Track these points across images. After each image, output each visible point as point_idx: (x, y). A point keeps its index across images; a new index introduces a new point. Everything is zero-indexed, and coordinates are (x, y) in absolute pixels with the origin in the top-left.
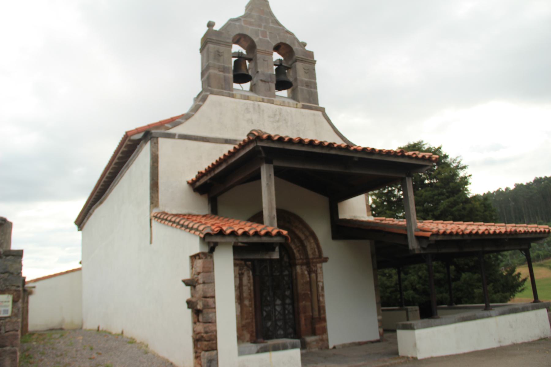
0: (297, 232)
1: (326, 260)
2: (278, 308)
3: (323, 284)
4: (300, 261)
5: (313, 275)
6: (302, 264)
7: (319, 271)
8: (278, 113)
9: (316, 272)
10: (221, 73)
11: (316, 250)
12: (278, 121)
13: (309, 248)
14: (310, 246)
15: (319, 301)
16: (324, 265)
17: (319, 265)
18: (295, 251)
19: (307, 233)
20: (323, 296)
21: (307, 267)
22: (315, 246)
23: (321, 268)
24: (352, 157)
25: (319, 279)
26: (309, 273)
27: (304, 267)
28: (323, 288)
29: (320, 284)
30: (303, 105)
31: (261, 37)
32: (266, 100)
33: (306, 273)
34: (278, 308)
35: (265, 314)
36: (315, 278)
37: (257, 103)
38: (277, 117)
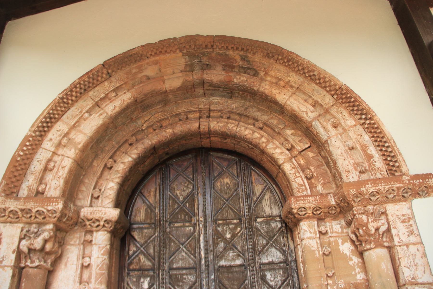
0: (282, 97)
4: (311, 203)
6: (320, 215)
7: (400, 233)
9: (385, 239)
11: (372, 150)
13: (337, 147)
14: (343, 140)
17: (391, 208)
18: (287, 168)
19: (328, 100)
21: (349, 224)
22: (367, 138)
23: (408, 220)
26: (359, 245)
33: (346, 248)
36: (386, 266)
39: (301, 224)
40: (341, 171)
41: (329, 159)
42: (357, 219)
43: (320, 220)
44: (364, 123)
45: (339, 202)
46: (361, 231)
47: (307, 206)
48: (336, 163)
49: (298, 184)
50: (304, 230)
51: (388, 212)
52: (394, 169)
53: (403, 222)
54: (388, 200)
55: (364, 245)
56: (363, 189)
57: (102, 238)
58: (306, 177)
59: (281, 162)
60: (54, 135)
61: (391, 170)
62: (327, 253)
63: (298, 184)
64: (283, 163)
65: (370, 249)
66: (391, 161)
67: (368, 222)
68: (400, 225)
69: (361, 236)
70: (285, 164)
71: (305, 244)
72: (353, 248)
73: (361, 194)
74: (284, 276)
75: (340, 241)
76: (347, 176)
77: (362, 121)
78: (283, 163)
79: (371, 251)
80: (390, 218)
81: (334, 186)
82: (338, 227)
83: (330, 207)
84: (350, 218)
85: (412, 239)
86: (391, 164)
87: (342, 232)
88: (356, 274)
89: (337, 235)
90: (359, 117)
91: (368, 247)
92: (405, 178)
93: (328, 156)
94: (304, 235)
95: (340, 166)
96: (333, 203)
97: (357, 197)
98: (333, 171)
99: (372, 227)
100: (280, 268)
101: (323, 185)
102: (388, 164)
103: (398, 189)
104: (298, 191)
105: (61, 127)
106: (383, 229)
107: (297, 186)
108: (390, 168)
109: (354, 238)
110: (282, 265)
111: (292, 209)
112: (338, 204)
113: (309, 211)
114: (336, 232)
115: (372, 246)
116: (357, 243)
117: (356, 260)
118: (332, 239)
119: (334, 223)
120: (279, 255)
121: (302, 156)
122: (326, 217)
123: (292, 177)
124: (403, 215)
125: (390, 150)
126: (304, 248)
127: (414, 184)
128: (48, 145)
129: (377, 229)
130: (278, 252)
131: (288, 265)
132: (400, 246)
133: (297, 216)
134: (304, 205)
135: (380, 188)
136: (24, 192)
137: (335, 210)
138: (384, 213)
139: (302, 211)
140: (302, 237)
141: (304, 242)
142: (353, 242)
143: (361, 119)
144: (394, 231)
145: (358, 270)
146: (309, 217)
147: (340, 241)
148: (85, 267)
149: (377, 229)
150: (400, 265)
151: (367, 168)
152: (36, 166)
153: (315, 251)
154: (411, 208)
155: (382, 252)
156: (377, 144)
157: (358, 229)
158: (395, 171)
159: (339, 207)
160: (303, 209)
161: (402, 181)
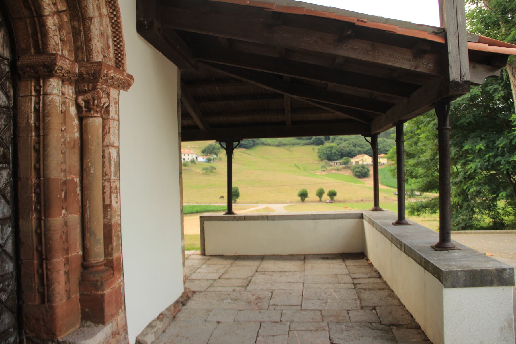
1: (126, 84)
5: (96, 122)
15: (107, 207)
20: (118, 190)
21: (78, 93)
23: (117, 103)
25: (112, 138)
27: (70, 91)
33: (73, 110)
39: (52, 80)
40: (93, 49)
41: (82, 33)
42: (98, 92)
43: (63, 81)
44: (112, 18)
45: (84, 73)
46: (96, 102)
47: (65, 66)
48: (91, 40)
49: (56, 43)
50: (54, 86)
51: (111, 94)
52: (120, 64)
53: (115, 103)
54: (112, 86)
55: (92, 112)
56: (110, 72)
58: (60, 38)
59: (47, 13)
61: (117, 64)
62: (63, 111)
63: (56, 43)
64: (49, 16)
65: (96, 117)
66: (120, 57)
67: (102, 97)
68: (113, 105)
69: (93, 104)
70: (50, 18)
71: (52, 99)
72: (76, 112)
73: (107, 75)
74: (7, 121)
75: (71, 104)
76: (97, 56)
77: (112, 16)
78: (49, 16)
79: (96, 119)
80: (111, 99)
81: (73, 55)
82: (71, 91)
83: (74, 73)
84: (87, 89)
85: (116, 117)
86: (120, 59)
87: (72, 97)
88: (75, 133)
89: (69, 98)
90: (111, 11)
91: (96, 115)
92: (125, 74)
93: (82, 30)
94: (52, 90)
95: (94, 45)
96: (77, 71)
97: (104, 76)
98: (79, 44)
99: (104, 100)
100: (4, 113)
101: (69, 51)
102: (117, 59)
103: (121, 79)
104: (54, 49)
106: (107, 105)
107: (54, 43)
108: (118, 62)
109: (83, 104)
110: (5, 109)
111: (56, 65)
112: (80, 74)
113: (63, 72)
114: (70, 96)
115: (99, 115)
116: (84, 109)
117: (76, 122)
118: (67, 100)
119: (70, 87)
120: (5, 99)
121: (60, 16)
122: (67, 80)
123: (52, 33)
124: (115, 99)
125: (122, 48)
126: (50, 102)
127: (127, 80)
129: (104, 104)
130: (4, 97)
131: (9, 111)
132: (112, 119)
133: (54, 72)
134: (62, 65)
135: (116, 75)
137: (75, 77)
138: (108, 94)
139: (59, 69)
140: (49, 91)
141: (51, 97)
142: (78, 107)
143: (112, 13)
144: (111, 108)
145: (76, 129)
146: (59, 77)
147: (71, 104)
149: (104, 104)
150: (109, 132)
151: (106, 55)
153: (57, 106)
154: (119, 95)
155: (100, 120)
156: (115, 39)
157: (94, 100)
158: (120, 66)
159: (79, 76)
160: (61, 68)
161: (123, 76)
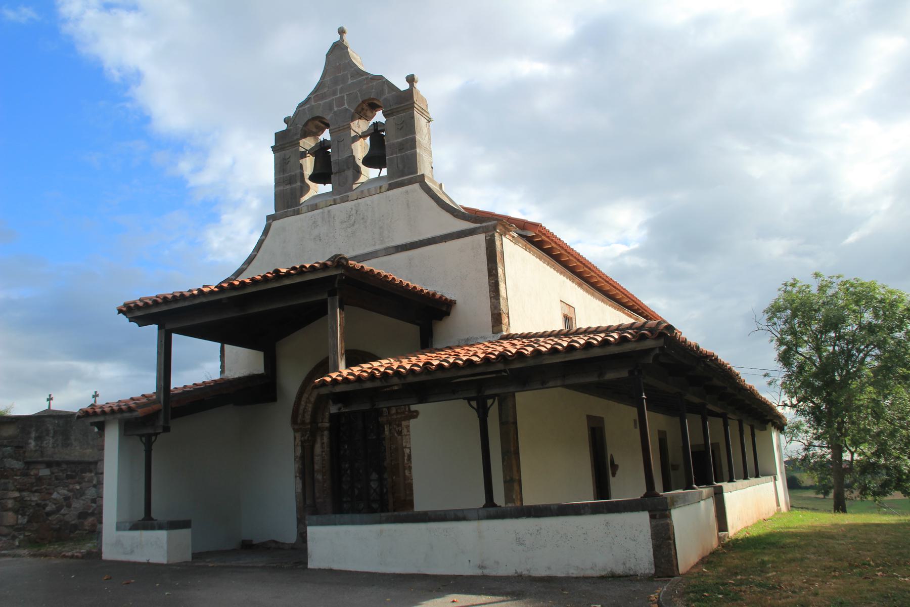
2: (374, 485)
3: (410, 448)
7: (405, 431)
8: (354, 212)
10: (288, 187)
12: (353, 225)
16: (412, 422)
17: (404, 423)
20: (410, 468)
24: (221, 299)
28: (410, 456)
29: (407, 451)
30: (390, 185)
31: (336, 109)
32: (338, 201)
34: (374, 485)
35: (356, 492)
37: (326, 209)
38: (353, 218)
57: (326, 433)
60: (304, 399)
105: (306, 395)
128: (303, 403)
136: (299, 421)
148: (323, 443)
152: (301, 411)
